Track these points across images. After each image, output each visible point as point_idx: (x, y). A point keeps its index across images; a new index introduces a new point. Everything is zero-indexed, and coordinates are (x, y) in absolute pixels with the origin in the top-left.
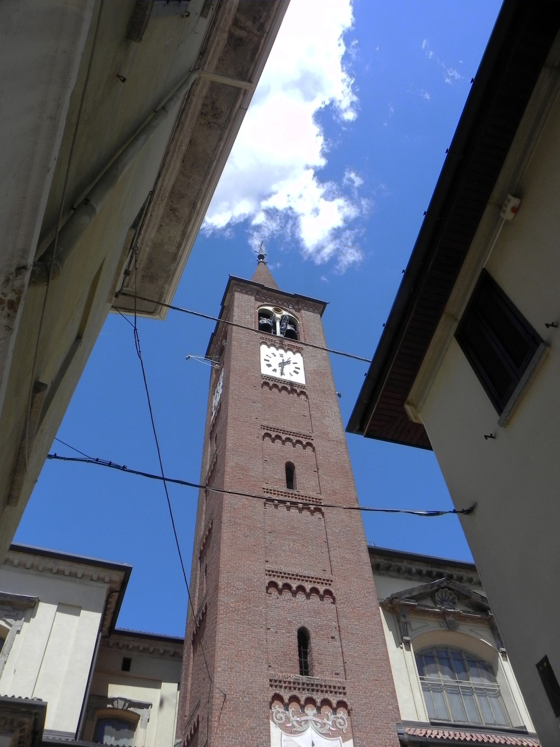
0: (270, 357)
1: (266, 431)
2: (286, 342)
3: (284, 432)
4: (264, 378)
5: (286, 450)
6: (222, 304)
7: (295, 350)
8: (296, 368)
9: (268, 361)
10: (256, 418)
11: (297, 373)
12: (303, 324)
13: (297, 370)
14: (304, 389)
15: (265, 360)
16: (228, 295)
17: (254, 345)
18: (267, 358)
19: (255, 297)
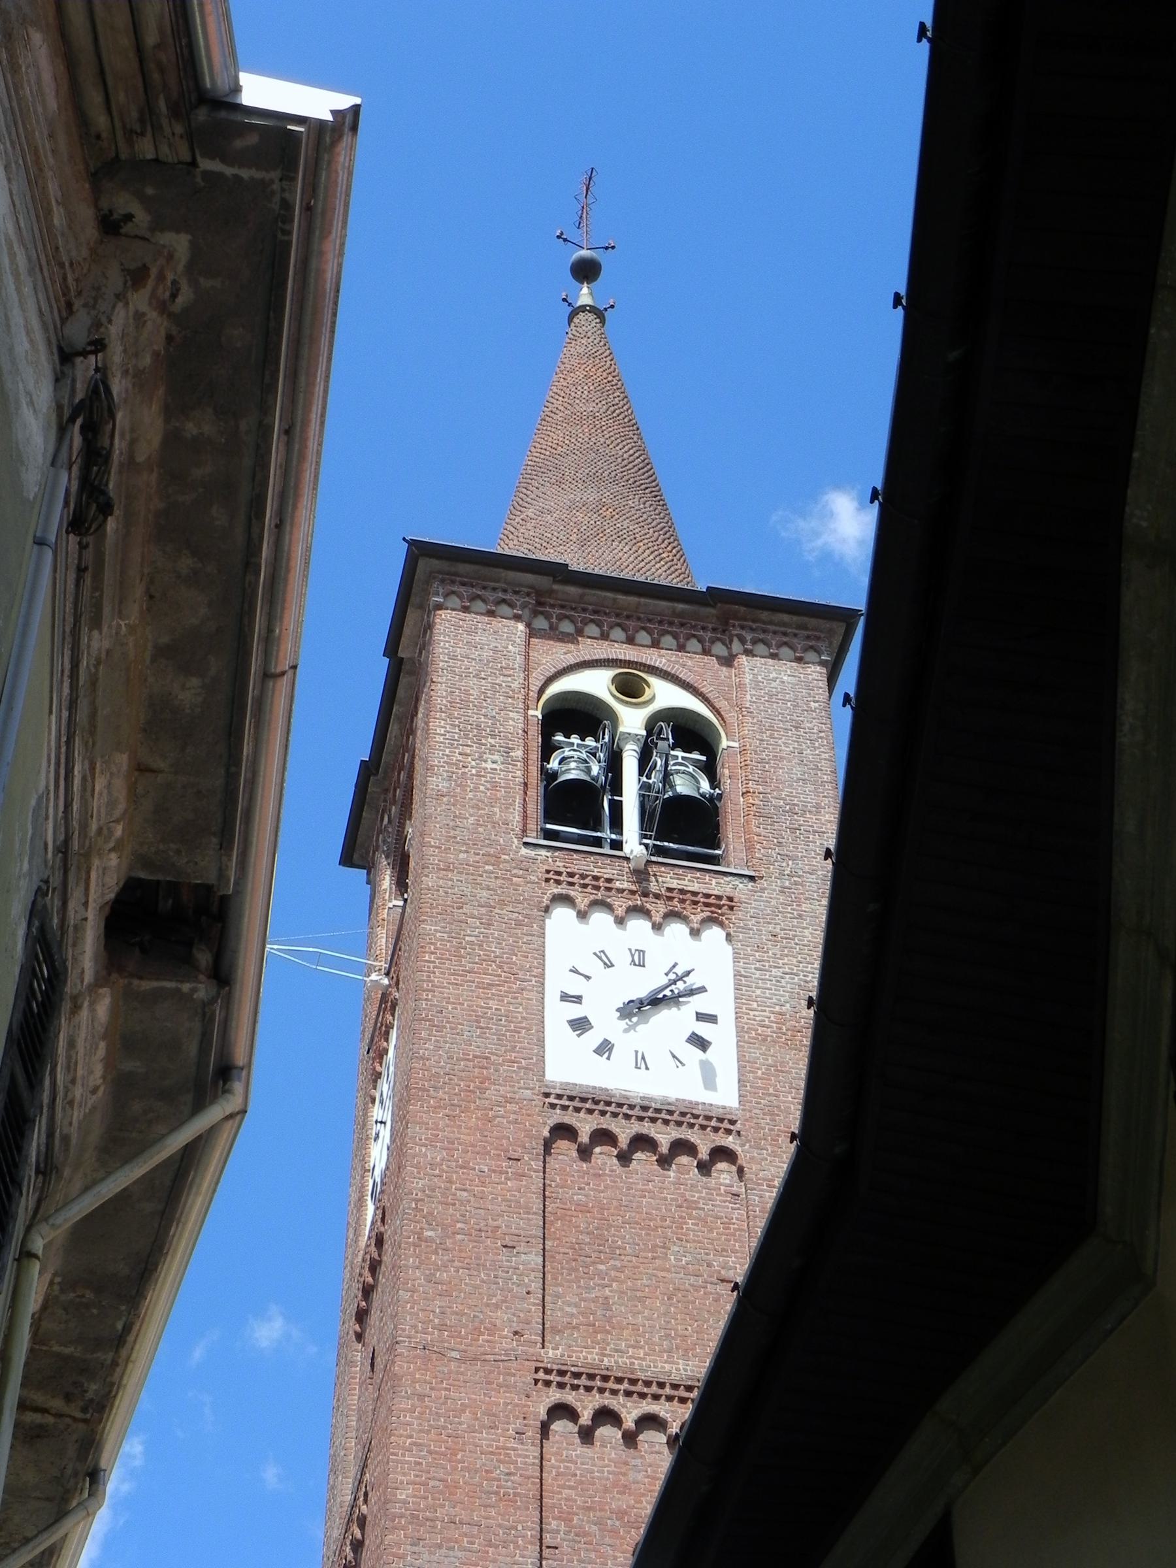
0: (588, 978)
1: (555, 1396)
2: (667, 878)
3: (636, 1386)
4: (553, 1106)
5: (640, 1477)
6: (392, 648)
7: (699, 917)
8: (701, 1017)
9: (578, 999)
10: (516, 1333)
11: (700, 1043)
12: (743, 751)
13: (704, 1029)
14: (728, 1132)
15: (565, 997)
16: (412, 616)
17: (519, 924)
18: (575, 986)
19: (528, 625)
